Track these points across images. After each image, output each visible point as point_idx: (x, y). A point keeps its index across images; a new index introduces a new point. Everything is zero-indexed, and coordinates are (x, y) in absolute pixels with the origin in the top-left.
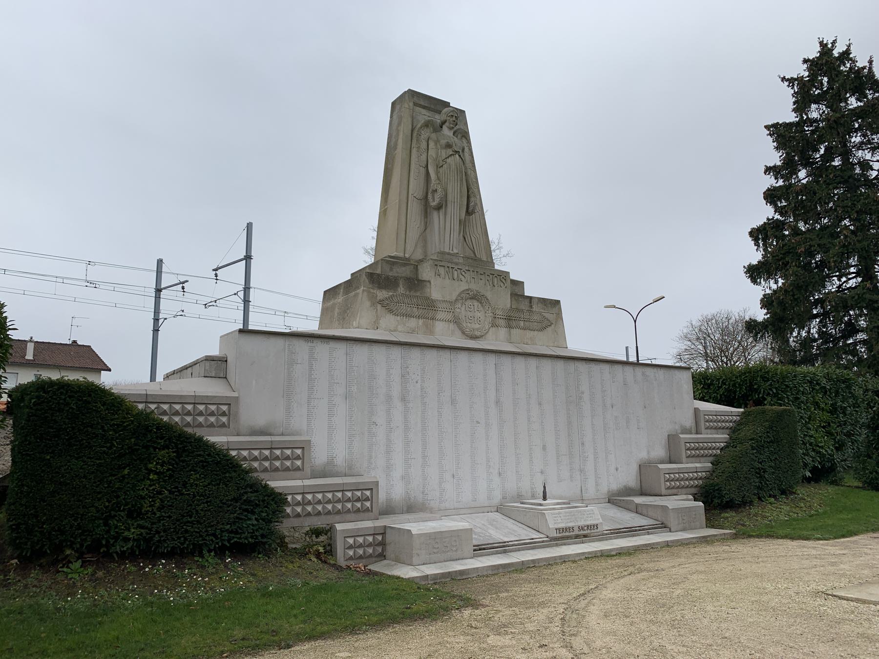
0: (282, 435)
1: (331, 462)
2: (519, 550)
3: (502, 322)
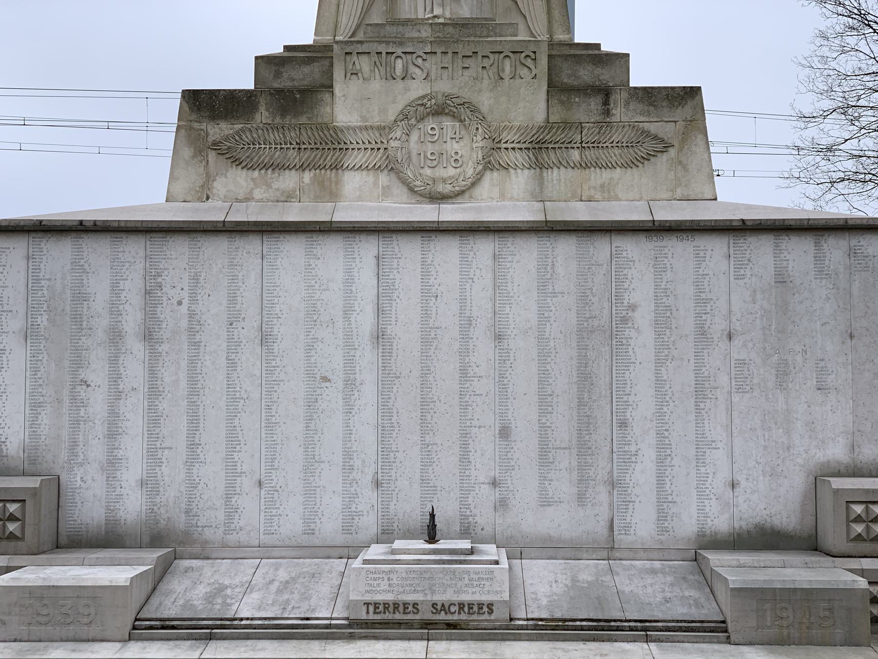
2: (248, 637)
3: (518, 157)
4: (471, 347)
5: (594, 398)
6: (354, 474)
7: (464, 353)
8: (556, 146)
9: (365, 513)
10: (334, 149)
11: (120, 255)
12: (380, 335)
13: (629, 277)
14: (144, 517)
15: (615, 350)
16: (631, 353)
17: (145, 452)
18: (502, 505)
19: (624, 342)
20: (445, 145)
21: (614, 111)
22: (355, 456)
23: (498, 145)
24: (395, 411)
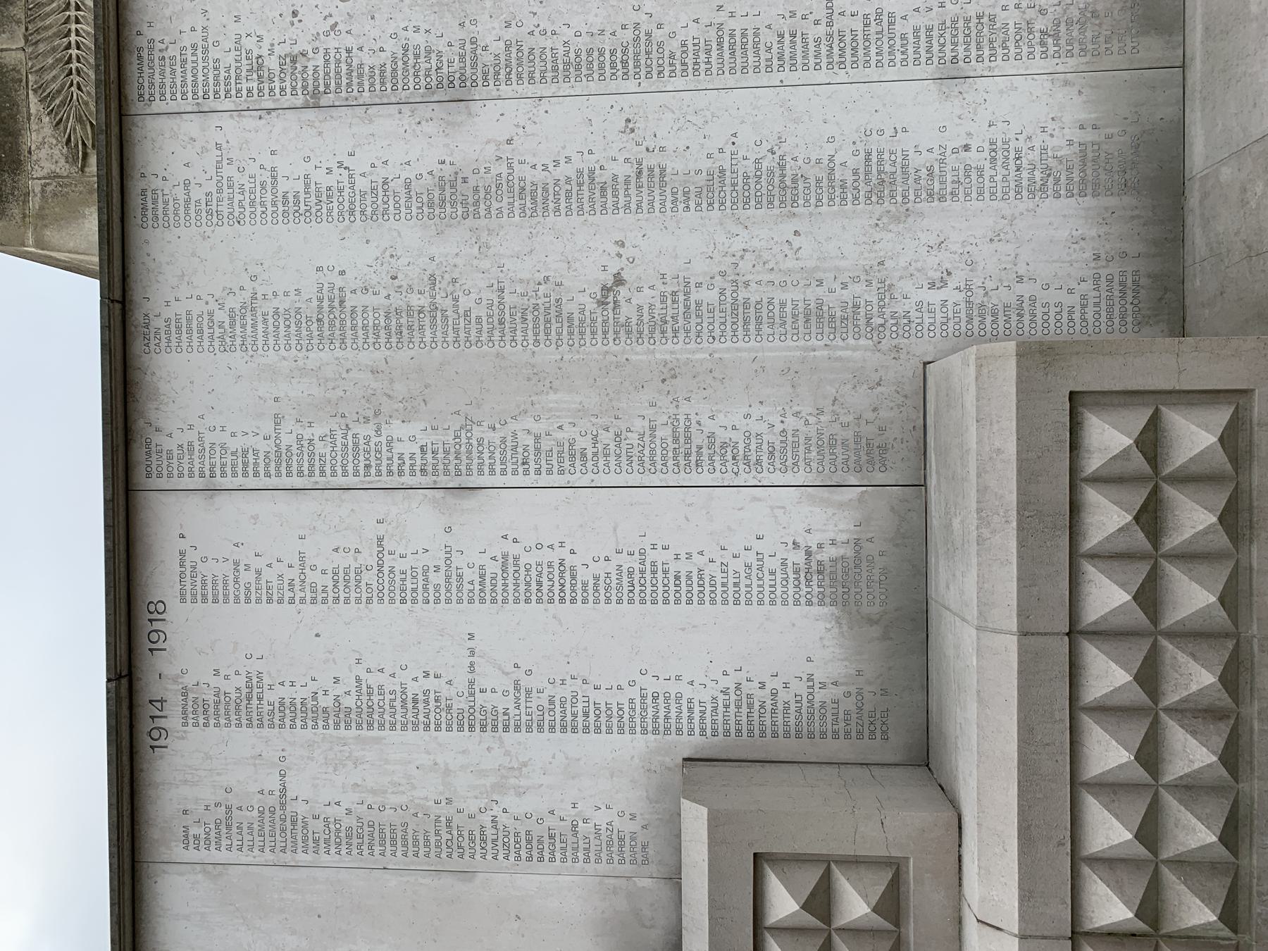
0: (674, 879)
1: (834, 581)
11: (197, 194)
14: (1071, 63)
17: (842, 76)
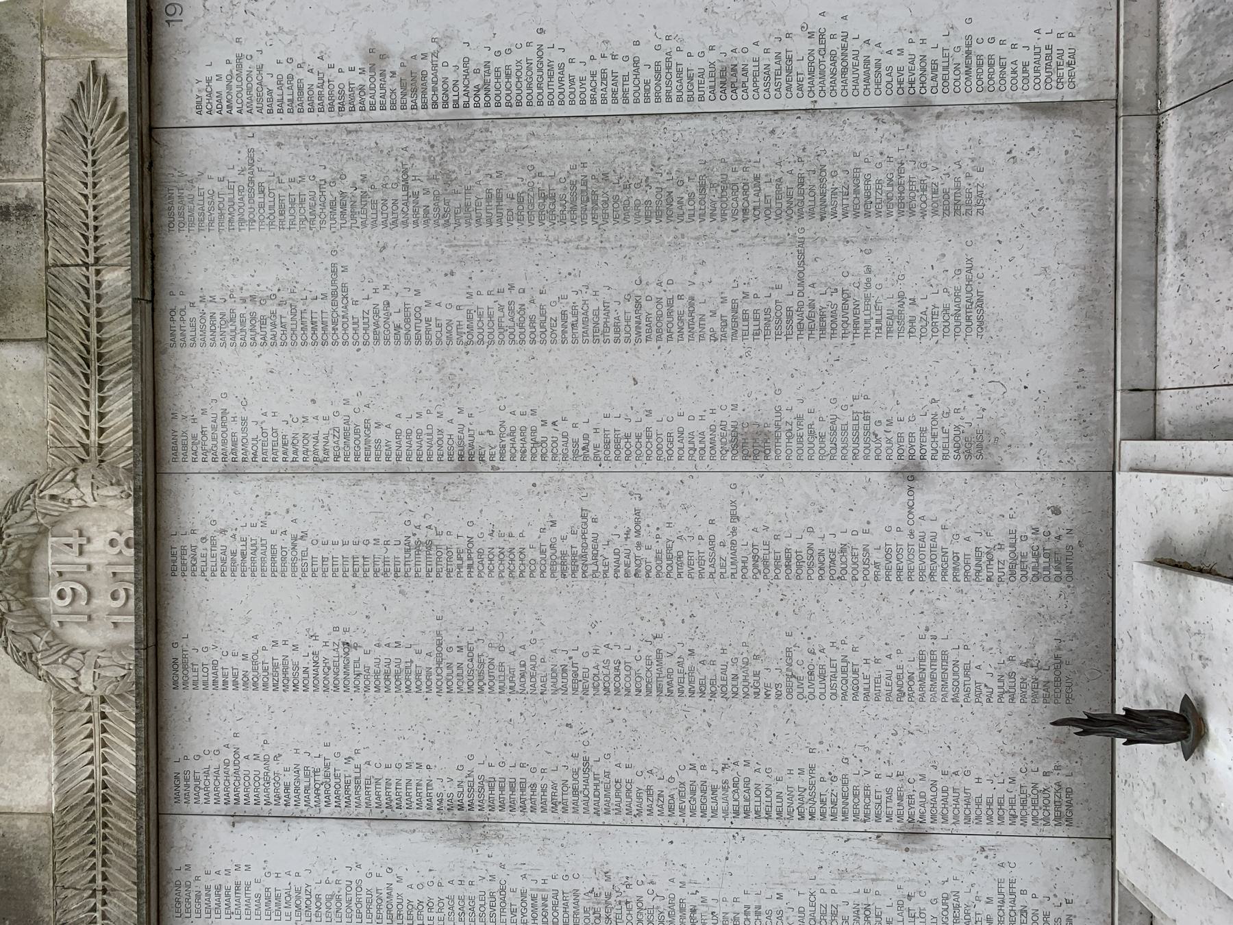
4: (498, 543)
5: (646, 170)
6: (881, 904)
7: (510, 562)
8: (94, 321)
9: (1004, 874)
10: (104, 813)
12: (459, 815)
13: (285, 70)
15: (504, 110)
16: (511, 60)
18: (978, 450)
19: (477, 81)
20: (96, 569)
21: (22, 195)
22: (830, 900)
23: (93, 450)
24: (688, 776)
